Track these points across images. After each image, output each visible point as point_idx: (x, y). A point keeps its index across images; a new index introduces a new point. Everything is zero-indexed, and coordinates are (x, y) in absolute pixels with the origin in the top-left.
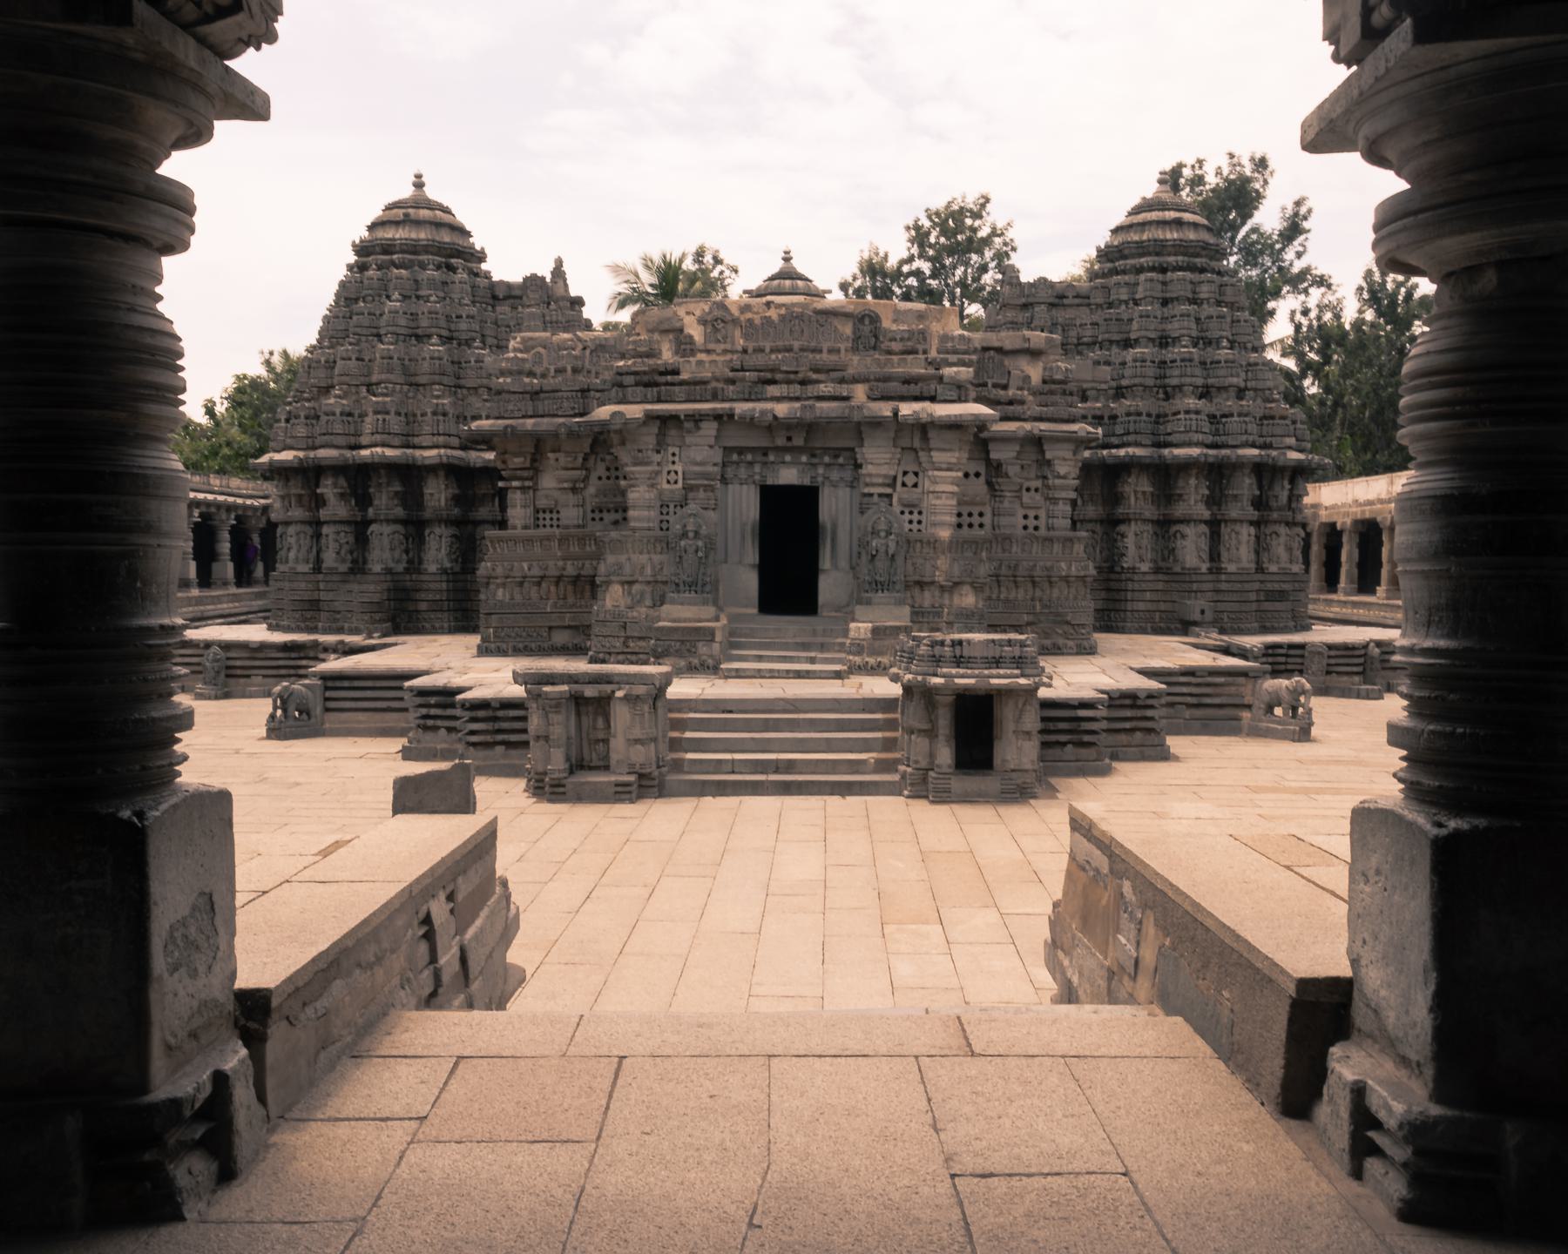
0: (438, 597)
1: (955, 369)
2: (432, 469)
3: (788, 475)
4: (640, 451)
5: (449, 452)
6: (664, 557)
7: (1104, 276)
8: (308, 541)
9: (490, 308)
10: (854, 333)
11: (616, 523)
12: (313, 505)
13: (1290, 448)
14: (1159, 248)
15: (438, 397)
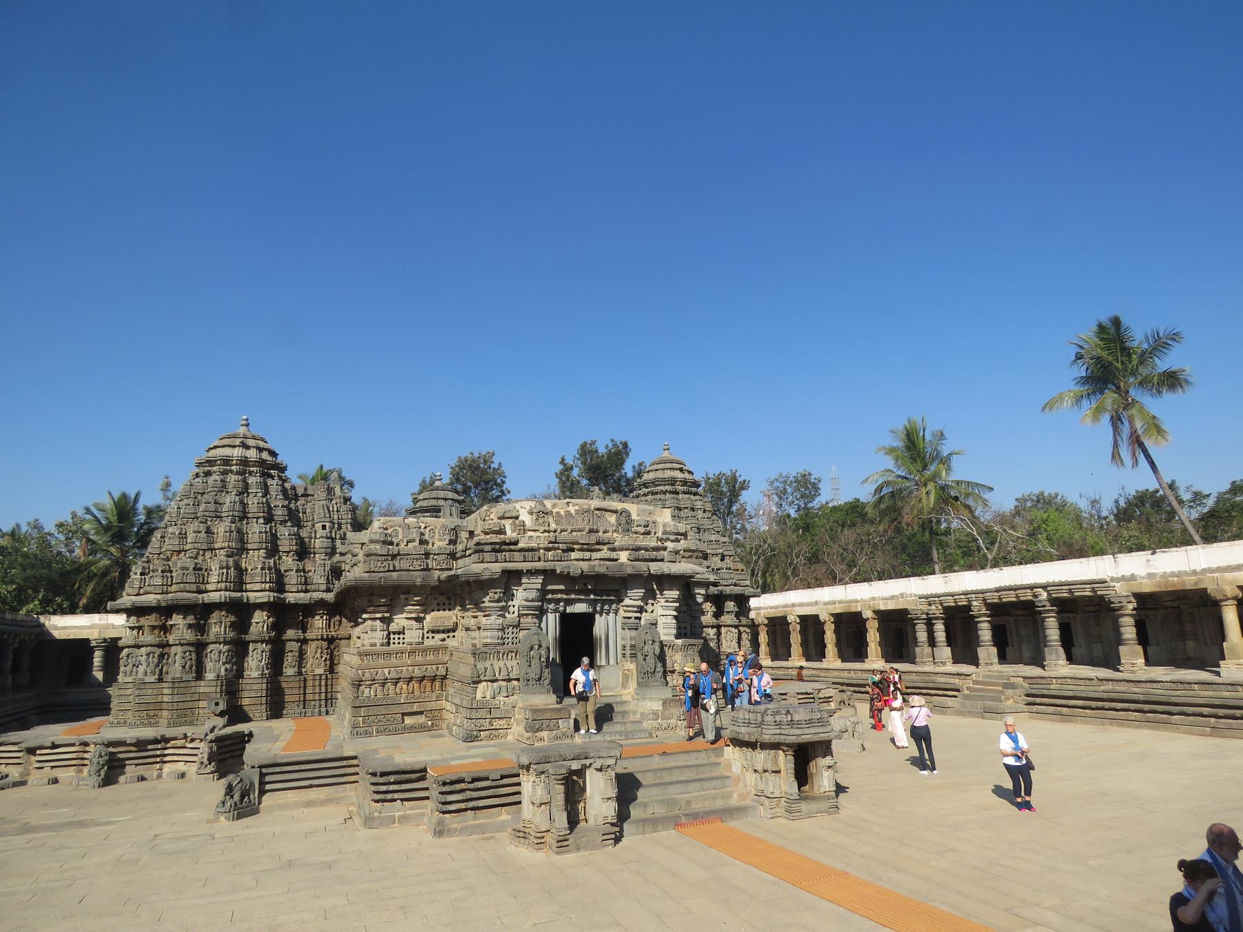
0: (259, 695)
1: (675, 543)
2: (261, 606)
3: (581, 608)
4: (496, 593)
5: (275, 594)
6: (514, 663)
7: (645, 495)
8: (156, 660)
9: (293, 501)
10: (617, 521)
11: (443, 640)
12: (162, 633)
13: (747, 586)
14: (673, 482)
15: (266, 558)
